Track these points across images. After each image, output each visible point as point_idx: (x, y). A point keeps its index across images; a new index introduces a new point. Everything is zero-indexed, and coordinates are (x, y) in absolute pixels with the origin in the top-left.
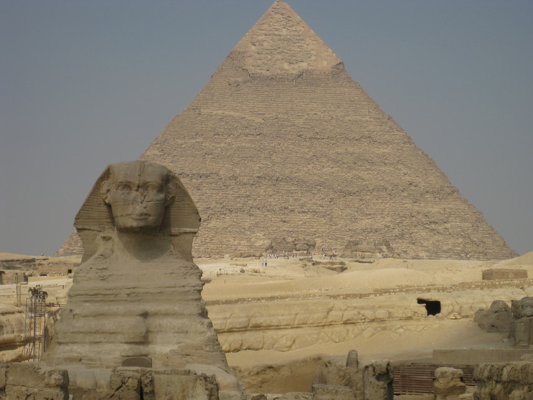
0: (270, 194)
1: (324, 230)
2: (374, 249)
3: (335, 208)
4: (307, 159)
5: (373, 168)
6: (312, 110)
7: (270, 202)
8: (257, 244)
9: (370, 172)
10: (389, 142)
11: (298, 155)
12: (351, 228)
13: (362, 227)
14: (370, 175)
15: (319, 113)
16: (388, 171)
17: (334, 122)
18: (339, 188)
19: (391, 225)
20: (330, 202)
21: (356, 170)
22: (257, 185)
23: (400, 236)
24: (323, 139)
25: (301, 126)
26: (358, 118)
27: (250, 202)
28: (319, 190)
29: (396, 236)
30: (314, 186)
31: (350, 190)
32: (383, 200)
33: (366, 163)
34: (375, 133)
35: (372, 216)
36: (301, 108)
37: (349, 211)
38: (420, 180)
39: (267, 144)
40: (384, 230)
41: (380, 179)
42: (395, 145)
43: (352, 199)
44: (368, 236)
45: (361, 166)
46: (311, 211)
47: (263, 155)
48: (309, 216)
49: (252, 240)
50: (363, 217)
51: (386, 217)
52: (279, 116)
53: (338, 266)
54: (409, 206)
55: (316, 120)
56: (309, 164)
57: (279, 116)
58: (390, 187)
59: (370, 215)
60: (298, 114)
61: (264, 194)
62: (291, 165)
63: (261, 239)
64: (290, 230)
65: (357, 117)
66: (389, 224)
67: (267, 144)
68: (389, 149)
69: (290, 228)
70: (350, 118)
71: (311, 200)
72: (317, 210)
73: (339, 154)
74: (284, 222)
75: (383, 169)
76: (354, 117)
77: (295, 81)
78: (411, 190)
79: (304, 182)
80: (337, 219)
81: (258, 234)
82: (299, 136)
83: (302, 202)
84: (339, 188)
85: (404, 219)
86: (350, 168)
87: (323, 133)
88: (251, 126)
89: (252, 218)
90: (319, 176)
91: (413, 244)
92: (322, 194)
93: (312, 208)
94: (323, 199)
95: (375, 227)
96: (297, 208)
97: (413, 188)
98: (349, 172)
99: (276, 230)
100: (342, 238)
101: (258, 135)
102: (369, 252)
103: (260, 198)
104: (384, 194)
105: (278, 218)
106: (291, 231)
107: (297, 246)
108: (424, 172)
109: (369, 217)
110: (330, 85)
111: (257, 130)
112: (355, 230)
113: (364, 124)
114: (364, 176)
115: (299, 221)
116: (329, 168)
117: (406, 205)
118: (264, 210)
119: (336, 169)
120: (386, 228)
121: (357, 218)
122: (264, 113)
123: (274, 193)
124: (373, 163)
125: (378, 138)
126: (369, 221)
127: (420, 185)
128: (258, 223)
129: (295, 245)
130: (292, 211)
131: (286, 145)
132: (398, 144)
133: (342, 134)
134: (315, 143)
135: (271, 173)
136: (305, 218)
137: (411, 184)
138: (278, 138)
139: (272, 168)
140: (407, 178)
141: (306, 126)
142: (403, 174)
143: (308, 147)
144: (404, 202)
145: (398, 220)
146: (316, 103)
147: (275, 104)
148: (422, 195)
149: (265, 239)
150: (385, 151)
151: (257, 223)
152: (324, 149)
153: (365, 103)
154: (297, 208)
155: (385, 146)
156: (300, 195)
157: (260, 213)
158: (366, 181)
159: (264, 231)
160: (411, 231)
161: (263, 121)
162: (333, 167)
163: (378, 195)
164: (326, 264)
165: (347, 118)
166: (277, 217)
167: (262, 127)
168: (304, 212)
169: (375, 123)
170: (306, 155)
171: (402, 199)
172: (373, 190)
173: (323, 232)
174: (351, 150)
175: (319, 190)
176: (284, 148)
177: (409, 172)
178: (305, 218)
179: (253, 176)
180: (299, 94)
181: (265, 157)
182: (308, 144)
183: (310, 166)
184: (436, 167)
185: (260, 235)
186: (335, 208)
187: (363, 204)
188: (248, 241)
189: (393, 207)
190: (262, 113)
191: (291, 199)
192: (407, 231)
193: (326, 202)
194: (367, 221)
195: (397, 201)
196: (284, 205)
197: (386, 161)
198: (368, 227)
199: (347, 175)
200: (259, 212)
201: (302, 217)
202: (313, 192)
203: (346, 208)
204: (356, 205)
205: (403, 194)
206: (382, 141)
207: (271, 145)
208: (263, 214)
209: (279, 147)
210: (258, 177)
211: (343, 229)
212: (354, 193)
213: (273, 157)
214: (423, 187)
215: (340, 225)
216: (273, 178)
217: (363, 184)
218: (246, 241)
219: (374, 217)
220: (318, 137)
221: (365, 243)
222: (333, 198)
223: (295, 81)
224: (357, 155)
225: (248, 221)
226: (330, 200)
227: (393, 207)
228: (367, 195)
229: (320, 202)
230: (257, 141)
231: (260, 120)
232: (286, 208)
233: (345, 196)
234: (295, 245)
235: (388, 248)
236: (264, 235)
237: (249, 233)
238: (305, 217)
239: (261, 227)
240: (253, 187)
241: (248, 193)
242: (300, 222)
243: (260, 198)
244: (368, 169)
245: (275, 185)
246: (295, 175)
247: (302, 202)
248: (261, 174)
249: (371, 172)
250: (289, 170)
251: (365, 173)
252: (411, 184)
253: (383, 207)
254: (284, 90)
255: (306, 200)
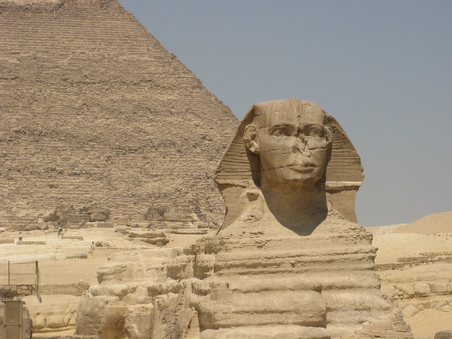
0: (33, 152)
1: (101, 196)
2: (184, 218)
3: (114, 169)
4: (76, 109)
5: (157, 119)
6: (78, 48)
7: (33, 163)
8: (20, 215)
9: (154, 123)
10: (175, 86)
11: (65, 104)
12: (134, 193)
13: (148, 191)
14: (153, 128)
15: (87, 52)
16: (176, 122)
17: (107, 63)
18: (117, 143)
19: (183, 189)
20: (107, 161)
21: (136, 121)
22: (15, 142)
23: (195, 202)
24: (94, 83)
25: (66, 68)
26: (136, 57)
27: (7, 163)
28: (92, 147)
29: (190, 202)
30: (86, 141)
31: (130, 146)
32: (171, 158)
33: (148, 112)
34: (157, 75)
35: (160, 178)
36: (64, 45)
37: (130, 171)
38: (215, 133)
39: (25, 91)
40: (175, 195)
41: (167, 132)
42: (182, 90)
43: (134, 157)
44: (156, 203)
45: (142, 116)
46: (84, 172)
47: (21, 104)
48: (82, 179)
49: (13, 210)
50: (149, 180)
51: (176, 178)
52: (38, 56)
53: (158, 238)
54: (203, 165)
55: (84, 60)
56: (78, 115)
57: (38, 56)
58: (179, 142)
59: (156, 176)
60: (60, 53)
61: (25, 152)
62: (56, 116)
63: (24, 208)
64: (60, 196)
65: (134, 56)
66: (180, 187)
67: (25, 91)
68: (175, 95)
69: (58, 194)
70: (125, 58)
71: (83, 159)
72: (92, 172)
73: (114, 102)
74: (52, 186)
75: (170, 119)
76: (130, 56)
77: (54, 12)
78: (205, 144)
79: (74, 137)
80: (116, 182)
81: (20, 203)
82: (65, 80)
83: (72, 161)
84: (117, 143)
85: (198, 180)
86: (129, 120)
87: (93, 76)
88: (5, 68)
89: (11, 183)
90: (91, 129)
91: (211, 211)
92: (96, 151)
93: (85, 168)
94: (98, 157)
95: (164, 191)
96: (65, 169)
97: (207, 142)
98: (128, 124)
99: (43, 197)
100: (124, 206)
101: (13, 79)
102: (180, 221)
103: (21, 158)
104: (172, 150)
105: (43, 182)
106: (61, 198)
107: (91, 216)
108: (219, 123)
109: (156, 179)
110: (99, 17)
111: (11, 73)
112: (140, 196)
113: (143, 65)
114: (147, 129)
115: (70, 185)
116: (104, 120)
117: (200, 163)
118: (25, 173)
119: (112, 120)
120: (178, 193)
121: (141, 181)
122: (19, 51)
123: (37, 151)
124: (156, 113)
125: (161, 81)
126: (157, 184)
127: (215, 139)
128: (19, 187)
129: (89, 214)
130: (61, 173)
131: (48, 91)
132: (186, 88)
133: (117, 77)
134: (84, 88)
135: (32, 126)
136: (77, 181)
137: (204, 138)
138: (39, 83)
139: (34, 120)
140: (199, 130)
141: (72, 68)
142: (194, 126)
143: (76, 94)
144: (197, 159)
145: (191, 182)
146: (82, 39)
147: (32, 41)
148: (218, 150)
149: (29, 208)
150: (170, 97)
151: (18, 189)
152: (95, 96)
153: (143, 39)
154: (66, 170)
155: (170, 92)
156: (70, 153)
157: (21, 175)
158: (149, 135)
159: (26, 198)
160: (207, 196)
161: (19, 62)
162: (108, 119)
163: (165, 152)
164: (143, 236)
165: (121, 58)
166: (42, 181)
167: (18, 70)
168: (75, 174)
169: (157, 63)
170: (74, 103)
171: (194, 156)
172: (159, 145)
173: (101, 198)
174: (129, 96)
175: (92, 147)
176: (46, 95)
177: (201, 123)
178: (77, 181)
179: (10, 131)
180: (61, 28)
181: (23, 107)
182: (76, 90)
183: (78, 117)
184: (233, 116)
185: (23, 203)
186: (114, 169)
187: (148, 163)
188: (8, 212)
189: (184, 166)
190: (16, 51)
191: (58, 158)
192: (202, 195)
193: (102, 161)
194: (153, 184)
195: (189, 159)
196: (50, 165)
197: (173, 110)
198: (156, 191)
199: (126, 128)
200: (19, 175)
201: (74, 181)
202: (85, 149)
203: (127, 168)
204: (139, 164)
205: (195, 150)
206: (166, 85)
207: (30, 91)
208: (25, 178)
209: (39, 93)
210: (16, 132)
211: (124, 194)
212: (136, 150)
213: (34, 107)
214: (219, 141)
215: (121, 189)
216: (35, 133)
217: (146, 138)
218: (5, 211)
219: (161, 179)
220: (88, 80)
221: (173, 210)
222: (111, 157)
223: (54, 12)
224: (136, 103)
225: (7, 186)
226: (106, 158)
227: (184, 166)
228: (152, 152)
229: (94, 162)
230: (12, 87)
231: (15, 61)
232: (53, 170)
233: (124, 154)
234: (89, 214)
235: (200, 216)
236: (28, 204)
237: (8, 201)
238: (77, 181)
239: (23, 194)
240: (11, 144)
241: (4, 152)
242: (72, 187)
243: (21, 158)
244: (151, 120)
245: (37, 141)
246: (62, 128)
247: (72, 161)
248: (20, 127)
249: (155, 124)
250: (54, 122)
251: (148, 125)
252: (204, 138)
253: (172, 167)
254: (42, 23)
255: (78, 159)
